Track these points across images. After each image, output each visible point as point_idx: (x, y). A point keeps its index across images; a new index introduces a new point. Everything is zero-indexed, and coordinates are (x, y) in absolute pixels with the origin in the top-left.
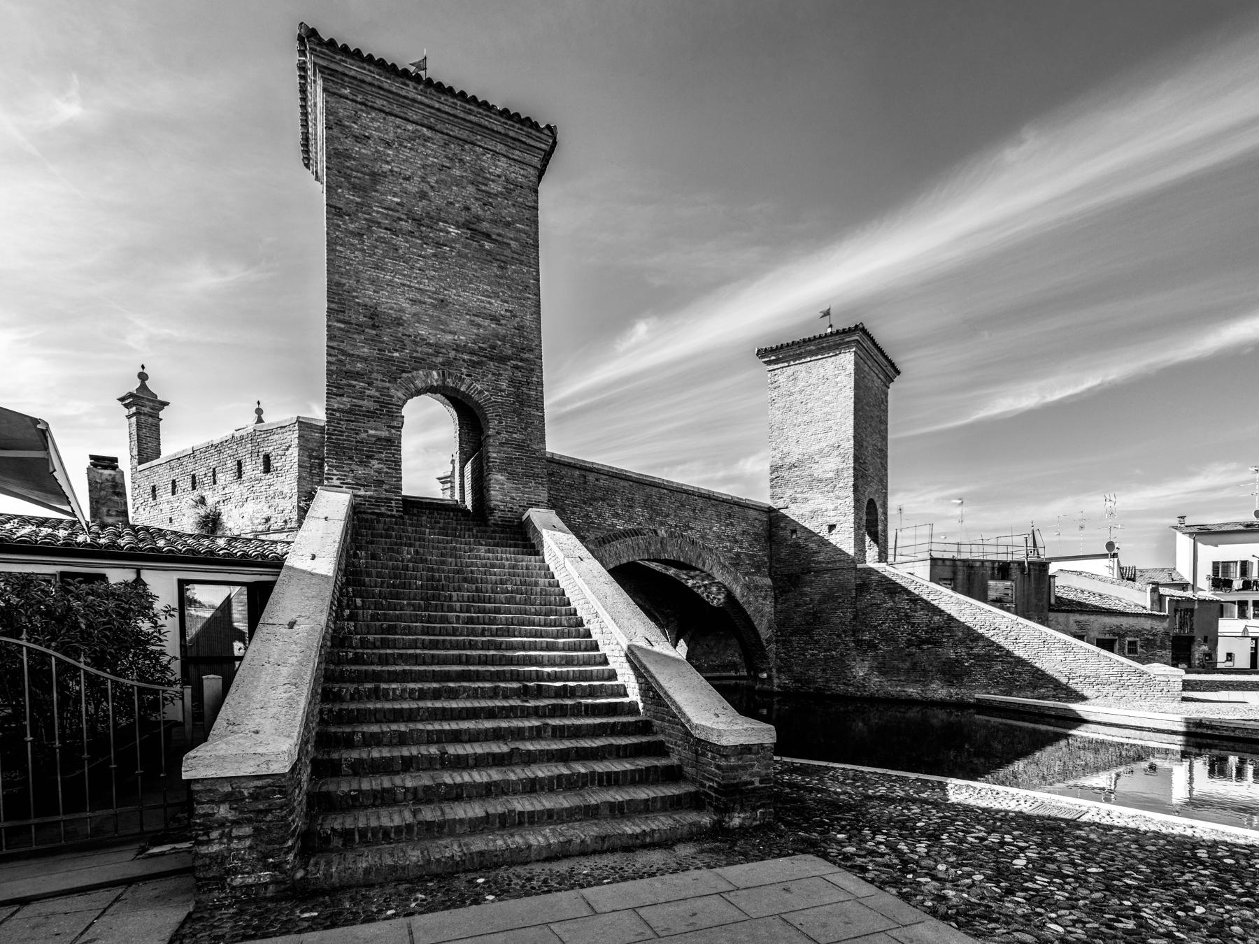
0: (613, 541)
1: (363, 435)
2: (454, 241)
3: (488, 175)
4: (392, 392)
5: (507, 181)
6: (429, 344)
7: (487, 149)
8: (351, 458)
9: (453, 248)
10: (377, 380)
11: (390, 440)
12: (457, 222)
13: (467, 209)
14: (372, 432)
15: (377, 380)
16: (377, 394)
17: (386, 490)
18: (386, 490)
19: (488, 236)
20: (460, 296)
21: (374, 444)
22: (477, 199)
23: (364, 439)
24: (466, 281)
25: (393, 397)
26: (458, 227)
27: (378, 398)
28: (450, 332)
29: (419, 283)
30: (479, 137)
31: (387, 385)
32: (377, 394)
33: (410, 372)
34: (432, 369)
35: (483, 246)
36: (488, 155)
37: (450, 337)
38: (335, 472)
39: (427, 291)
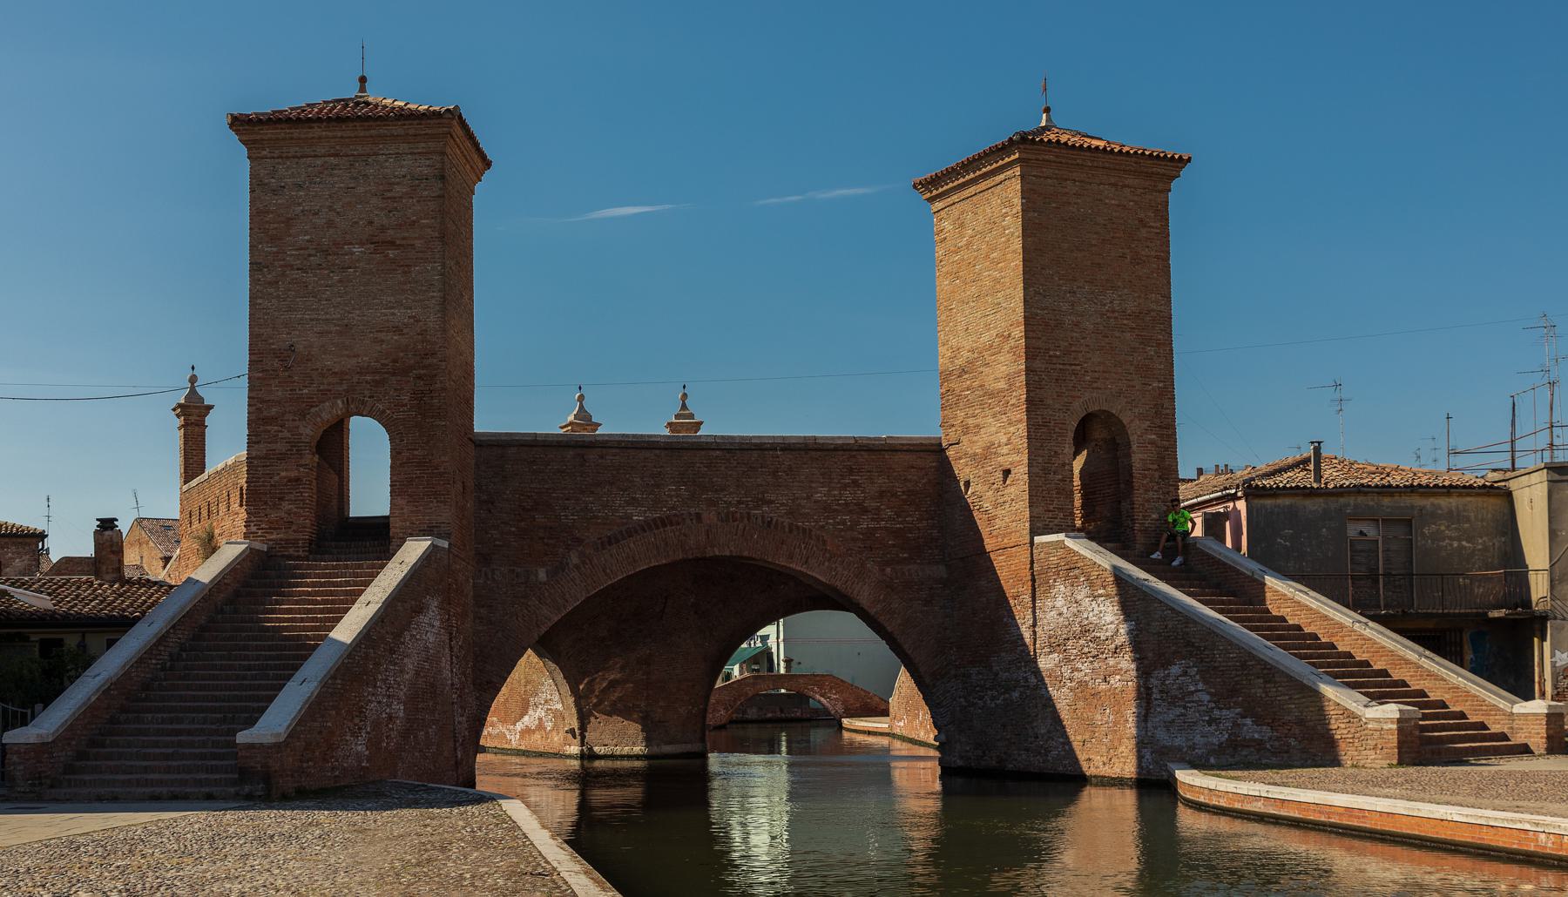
0: (658, 528)
1: (277, 478)
2: (358, 261)
3: (393, 180)
4: (302, 430)
5: (413, 178)
6: (336, 373)
7: (390, 154)
8: (266, 503)
9: (358, 267)
10: (288, 420)
11: (299, 479)
12: (361, 240)
13: (371, 223)
14: (283, 474)
15: (288, 420)
16: (289, 435)
17: (294, 531)
18: (294, 531)
19: (392, 244)
20: (364, 316)
21: (286, 485)
22: (382, 209)
23: (277, 482)
24: (370, 298)
25: (302, 435)
26: (362, 244)
27: (289, 438)
28: (354, 356)
29: (327, 313)
30: (381, 146)
31: (297, 423)
32: (289, 435)
33: (317, 406)
34: (337, 398)
35: (387, 256)
36: (391, 160)
37: (354, 361)
38: (253, 519)
39: (333, 320)
